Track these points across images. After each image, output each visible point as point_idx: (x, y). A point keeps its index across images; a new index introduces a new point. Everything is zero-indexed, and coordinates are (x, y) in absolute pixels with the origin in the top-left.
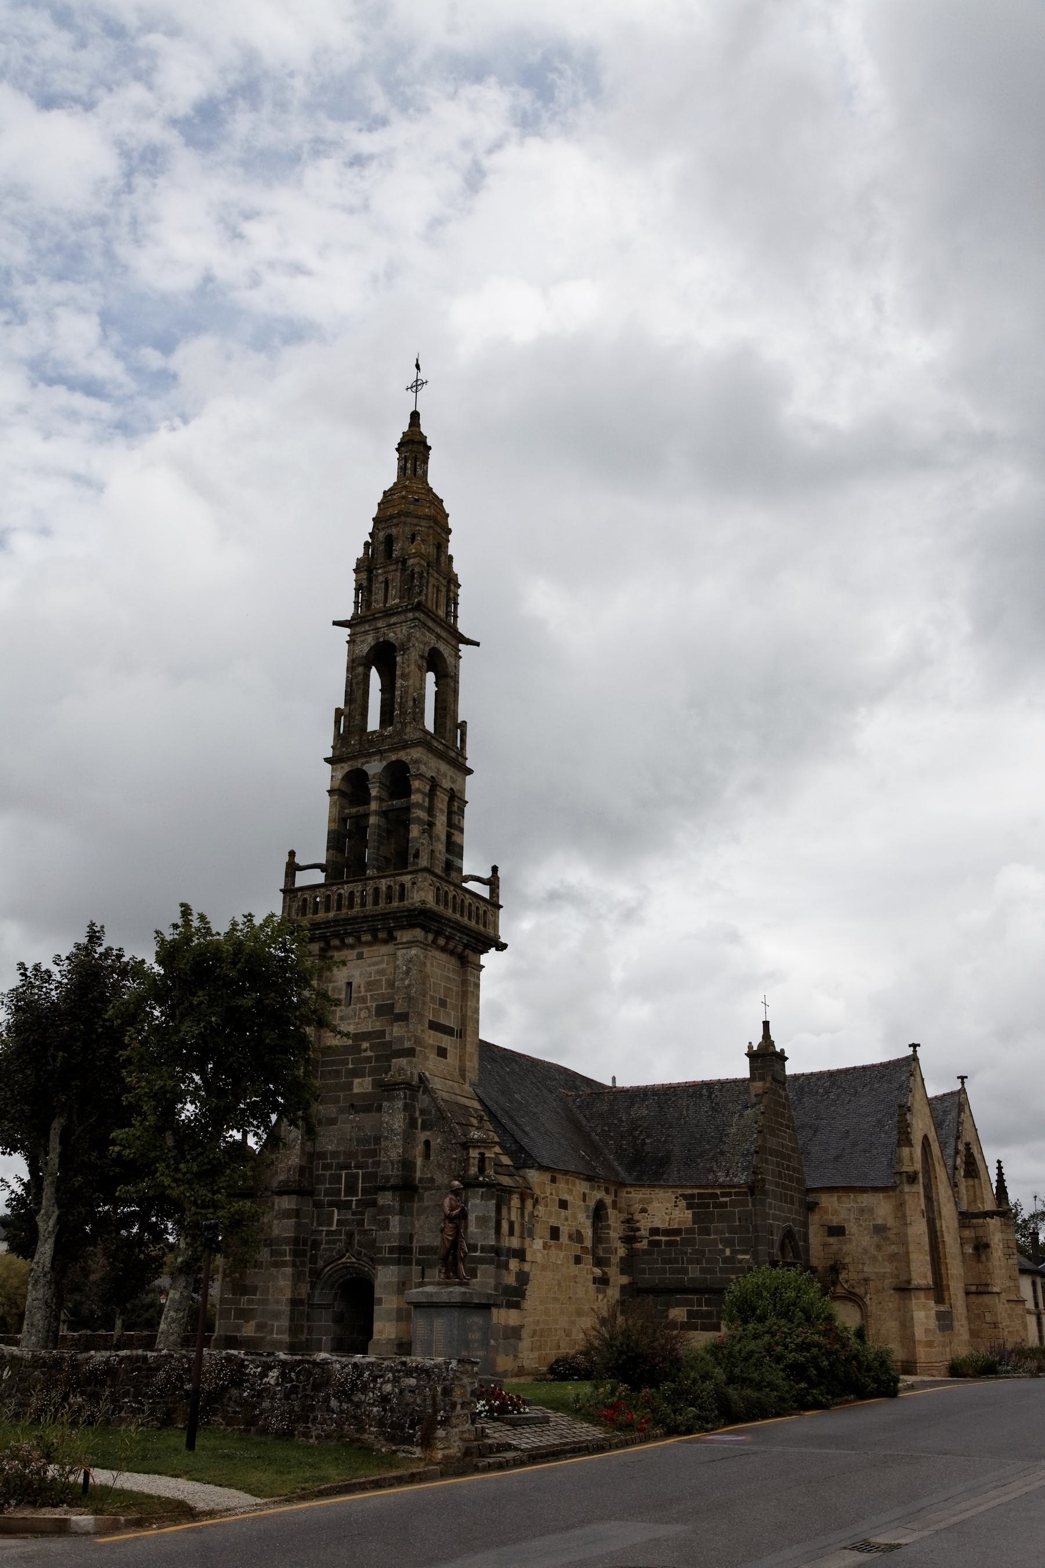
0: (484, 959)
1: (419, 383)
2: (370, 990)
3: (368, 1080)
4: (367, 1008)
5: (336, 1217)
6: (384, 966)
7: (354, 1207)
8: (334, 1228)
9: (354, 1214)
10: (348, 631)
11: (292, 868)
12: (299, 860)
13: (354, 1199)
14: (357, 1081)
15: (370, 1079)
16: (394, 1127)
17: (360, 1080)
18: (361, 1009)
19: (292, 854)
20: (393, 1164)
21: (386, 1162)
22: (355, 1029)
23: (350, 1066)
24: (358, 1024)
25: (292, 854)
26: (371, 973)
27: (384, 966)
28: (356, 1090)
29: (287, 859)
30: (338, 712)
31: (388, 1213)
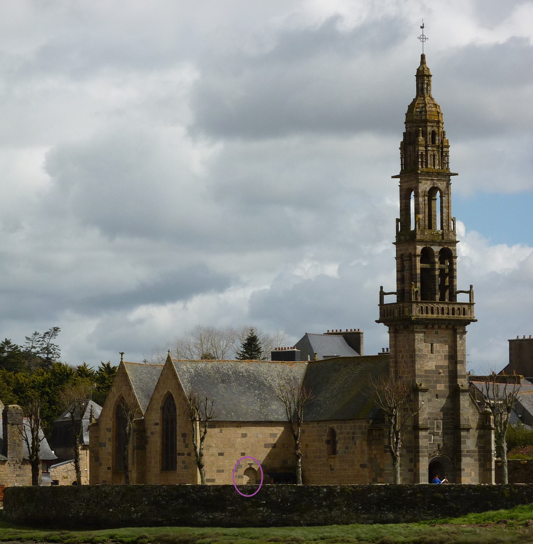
0: (468, 328)
1: (422, 37)
2: (442, 348)
3: (443, 385)
4: (441, 355)
5: (433, 438)
6: (446, 339)
7: (440, 434)
8: (432, 442)
9: (440, 437)
10: (399, 179)
11: (382, 294)
12: (385, 290)
13: (440, 431)
14: (438, 385)
15: (444, 384)
16: (466, 406)
17: (440, 385)
18: (438, 356)
19: (382, 288)
20: (465, 420)
21: (463, 419)
22: (436, 364)
23: (435, 379)
24: (437, 362)
25: (382, 288)
26: (441, 341)
27: (446, 339)
28: (438, 389)
29: (380, 290)
30: (398, 220)
31: (465, 438)
